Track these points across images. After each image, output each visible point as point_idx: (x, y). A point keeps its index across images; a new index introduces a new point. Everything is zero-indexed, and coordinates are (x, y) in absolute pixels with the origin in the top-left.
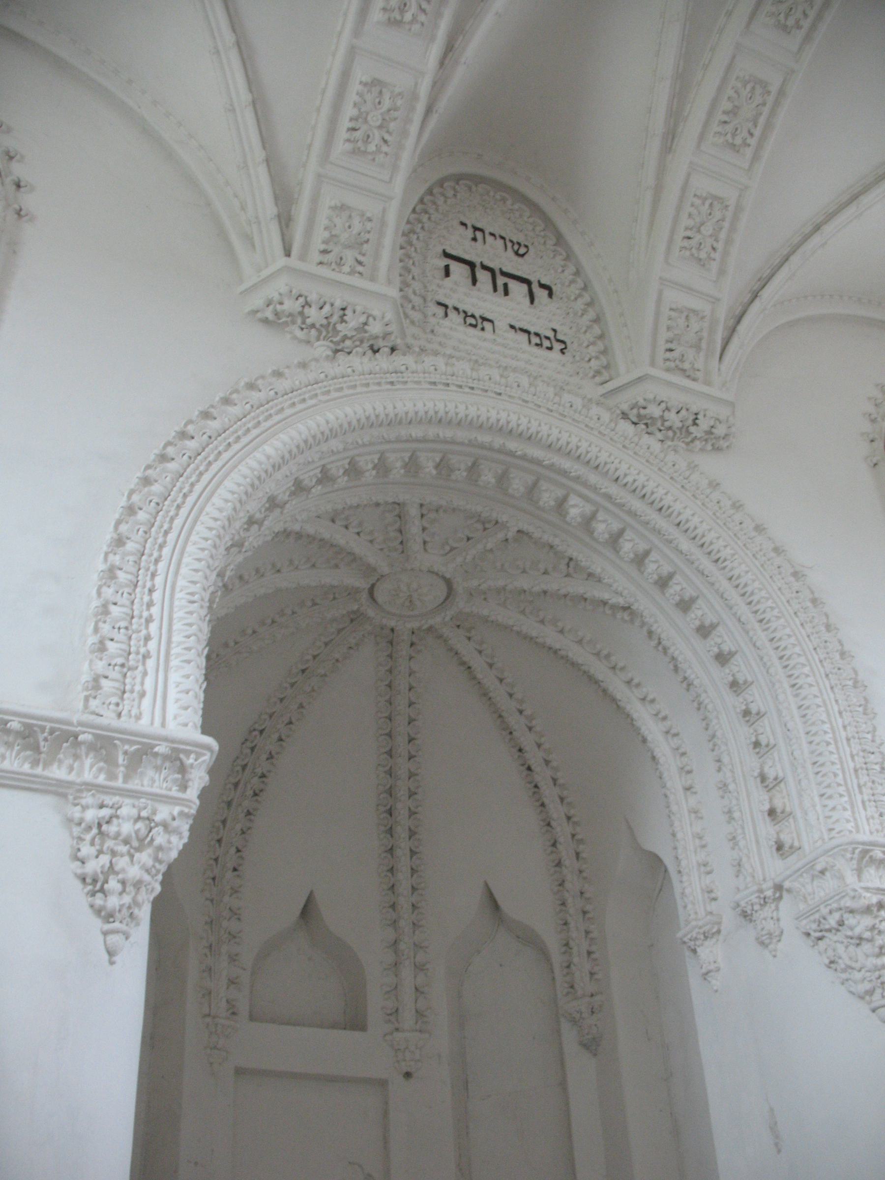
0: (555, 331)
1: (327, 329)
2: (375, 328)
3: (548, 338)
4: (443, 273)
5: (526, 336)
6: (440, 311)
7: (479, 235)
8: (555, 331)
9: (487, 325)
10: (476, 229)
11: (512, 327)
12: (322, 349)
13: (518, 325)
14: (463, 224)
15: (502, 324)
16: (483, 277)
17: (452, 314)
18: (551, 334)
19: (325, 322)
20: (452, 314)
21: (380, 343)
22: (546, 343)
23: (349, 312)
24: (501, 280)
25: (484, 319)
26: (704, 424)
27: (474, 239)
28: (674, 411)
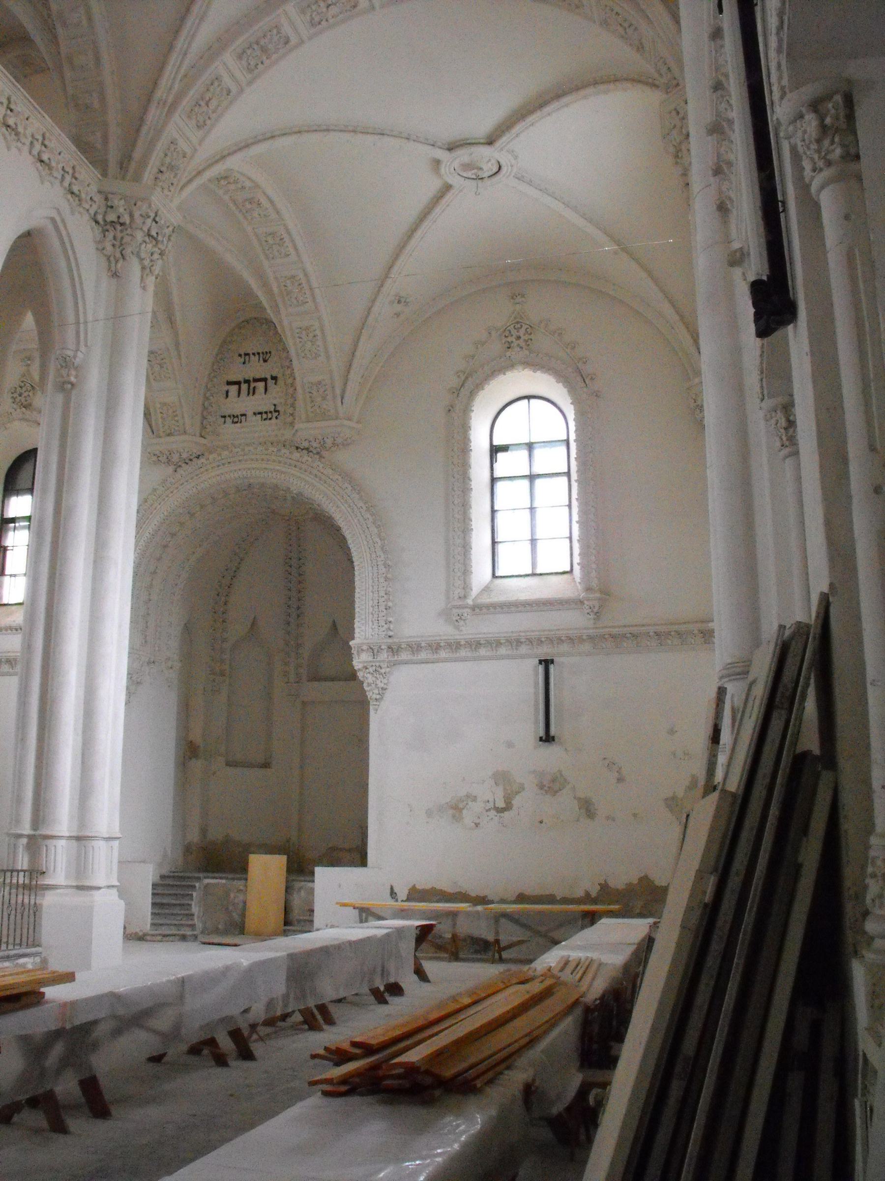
0: (275, 405)
1: (169, 462)
2: (184, 456)
3: (271, 412)
4: (225, 396)
5: (260, 415)
6: (223, 420)
7: (247, 357)
8: (275, 405)
9: (243, 418)
10: (246, 354)
11: (255, 414)
12: (171, 469)
13: (257, 411)
14: (240, 355)
15: (250, 414)
16: (244, 387)
17: (228, 419)
18: (272, 410)
19: (167, 460)
20: (228, 419)
21: (191, 457)
22: (270, 415)
23: (172, 454)
24: (253, 385)
25: (242, 415)
26: (329, 442)
27: (244, 363)
28: (313, 442)
